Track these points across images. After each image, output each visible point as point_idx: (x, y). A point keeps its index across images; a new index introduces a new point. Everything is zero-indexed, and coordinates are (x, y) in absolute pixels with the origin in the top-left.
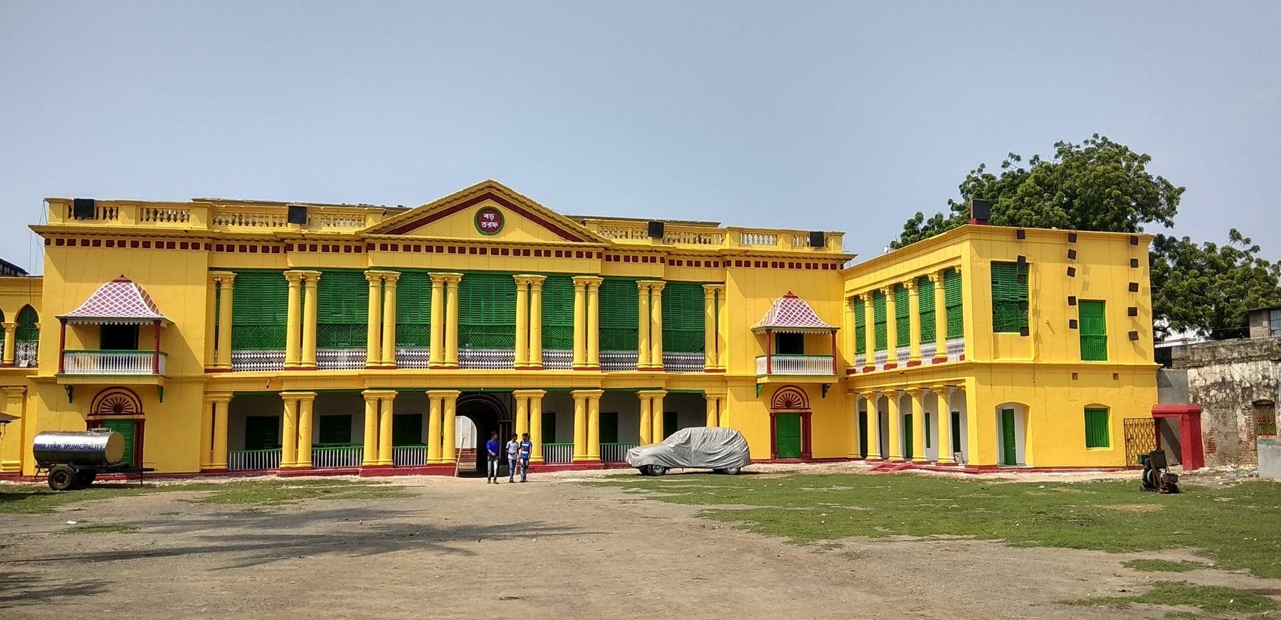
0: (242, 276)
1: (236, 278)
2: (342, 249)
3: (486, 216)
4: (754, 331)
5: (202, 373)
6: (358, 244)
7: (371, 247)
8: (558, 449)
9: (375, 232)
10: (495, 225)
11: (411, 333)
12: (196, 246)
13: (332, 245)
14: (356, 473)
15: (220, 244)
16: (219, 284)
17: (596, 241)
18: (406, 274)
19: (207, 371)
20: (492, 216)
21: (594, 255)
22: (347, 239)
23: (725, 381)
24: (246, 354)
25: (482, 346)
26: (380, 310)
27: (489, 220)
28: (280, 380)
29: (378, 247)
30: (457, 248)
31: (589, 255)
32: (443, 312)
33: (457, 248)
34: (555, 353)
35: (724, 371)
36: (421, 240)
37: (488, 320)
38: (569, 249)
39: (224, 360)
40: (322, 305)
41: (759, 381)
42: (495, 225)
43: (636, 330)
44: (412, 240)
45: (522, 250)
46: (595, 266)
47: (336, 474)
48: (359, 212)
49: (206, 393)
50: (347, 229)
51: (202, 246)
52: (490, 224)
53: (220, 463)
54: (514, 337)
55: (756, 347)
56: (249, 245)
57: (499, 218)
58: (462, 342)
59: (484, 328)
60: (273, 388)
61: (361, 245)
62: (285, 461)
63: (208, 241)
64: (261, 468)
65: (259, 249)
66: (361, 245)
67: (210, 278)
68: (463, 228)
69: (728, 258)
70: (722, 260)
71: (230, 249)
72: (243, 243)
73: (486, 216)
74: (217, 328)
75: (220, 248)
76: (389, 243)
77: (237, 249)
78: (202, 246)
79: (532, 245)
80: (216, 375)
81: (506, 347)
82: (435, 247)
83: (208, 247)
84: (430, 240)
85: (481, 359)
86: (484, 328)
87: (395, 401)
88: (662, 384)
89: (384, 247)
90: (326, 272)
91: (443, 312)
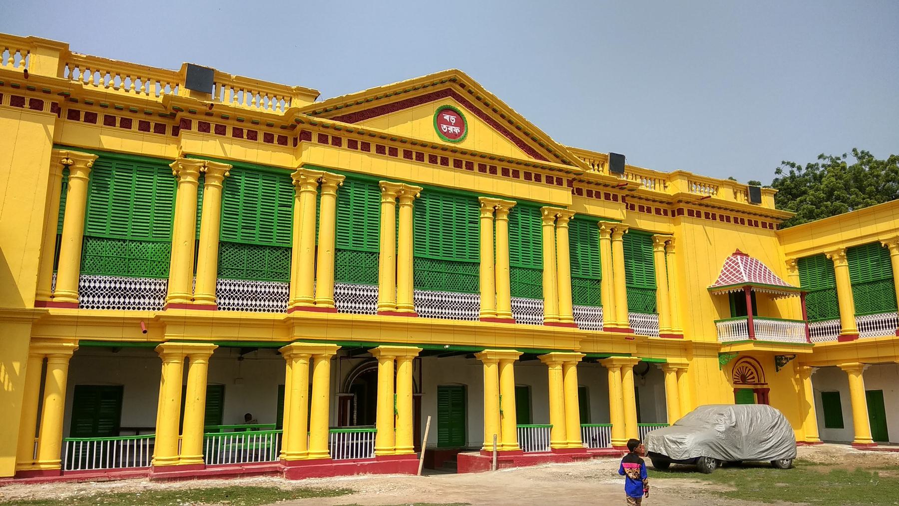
0: (105, 164)
1: (95, 164)
2: (261, 137)
3: (447, 117)
4: (710, 290)
5: (30, 305)
6: (284, 133)
7: (306, 136)
8: (535, 429)
9: (315, 114)
10: (457, 130)
11: (356, 263)
12: (37, 105)
13: (246, 128)
14: (275, 472)
15: (72, 106)
16: (67, 170)
17: (569, 164)
18: (355, 179)
19: (38, 304)
20: (453, 118)
21: (565, 183)
22: (270, 122)
23: (688, 348)
24: (103, 281)
25: (441, 288)
26: (311, 224)
27: (449, 124)
28: (160, 324)
29: (315, 138)
30: (415, 151)
31: (560, 182)
32: (396, 234)
33: (415, 151)
34: (525, 302)
35: (681, 336)
36: (372, 135)
37: (448, 253)
38: (538, 171)
39: (65, 284)
40: (227, 213)
41: (723, 350)
42: (457, 130)
43: (599, 281)
44: (361, 133)
45: (488, 165)
46: (561, 196)
47: (243, 474)
48: (286, 93)
49: (33, 339)
50: (277, 109)
51: (47, 106)
52: (451, 129)
53: (48, 456)
54: (477, 277)
55: (709, 310)
56: (120, 115)
57: (461, 122)
58: (418, 283)
59: (446, 267)
60: (152, 337)
61: (290, 133)
62: (163, 454)
63: (60, 99)
64: (109, 463)
65: (135, 125)
66: (290, 133)
67: (54, 158)
68: (419, 126)
69: (681, 205)
70: (673, 208)
71: (91, 118)
72: (111, 112)
73: (447, 117)
74: (59, 238)
75: (74, 115)
76: (330, 133)
77: (100, 119)
78: (47, 106)
79: (501, 159)
80: (53, 311)
81: (468, 291)
82: (389, 147)
83: (56, 108)
84: (383, 137)
85: (441, 305)
86: (446, 267)
87: (334, 359)
88: (633, 350)
89: (323, 139)
90: (240, 167)
91: (396, 234)
